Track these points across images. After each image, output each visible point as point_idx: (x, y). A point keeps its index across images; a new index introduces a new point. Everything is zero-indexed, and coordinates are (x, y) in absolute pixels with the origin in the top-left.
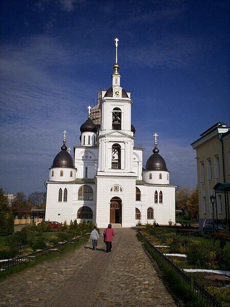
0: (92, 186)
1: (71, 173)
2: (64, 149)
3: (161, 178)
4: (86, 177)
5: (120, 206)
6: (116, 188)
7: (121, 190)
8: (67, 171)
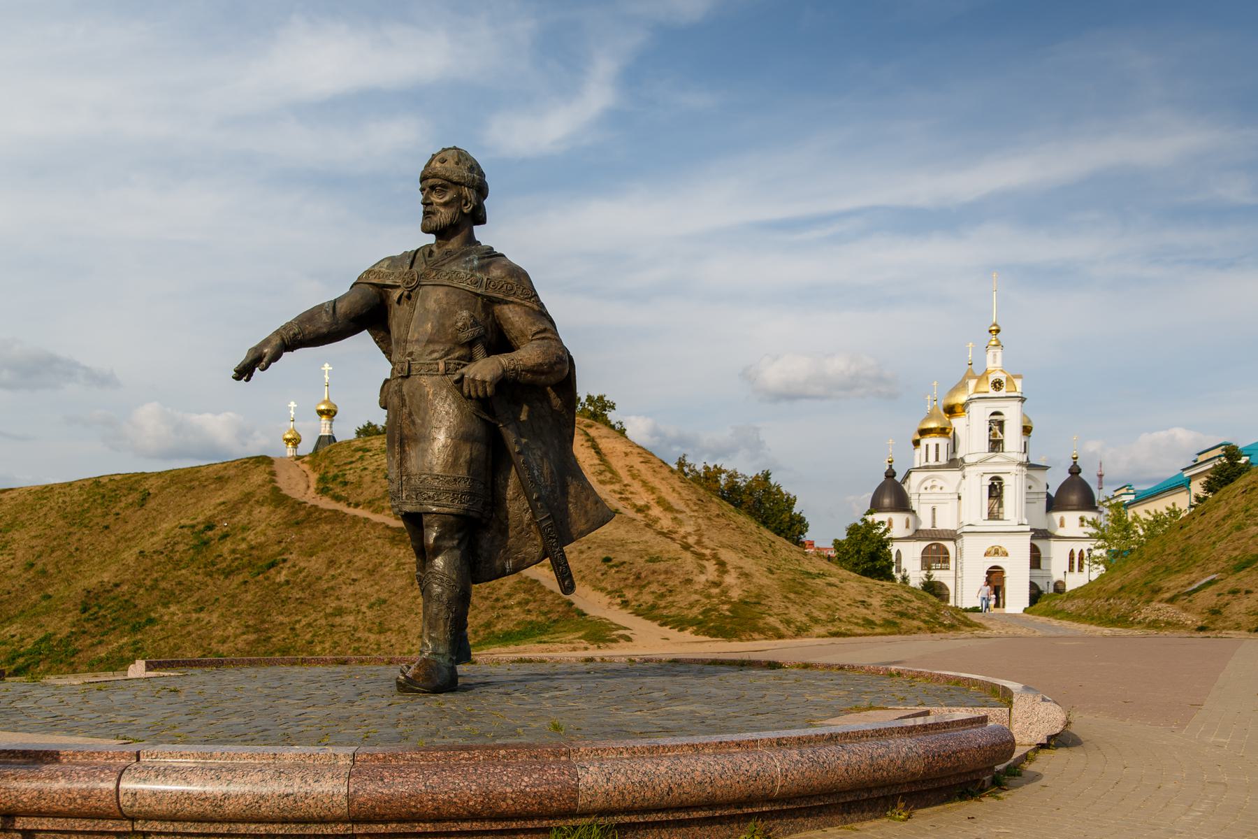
5: (1002, 579)
6: (997, 552)
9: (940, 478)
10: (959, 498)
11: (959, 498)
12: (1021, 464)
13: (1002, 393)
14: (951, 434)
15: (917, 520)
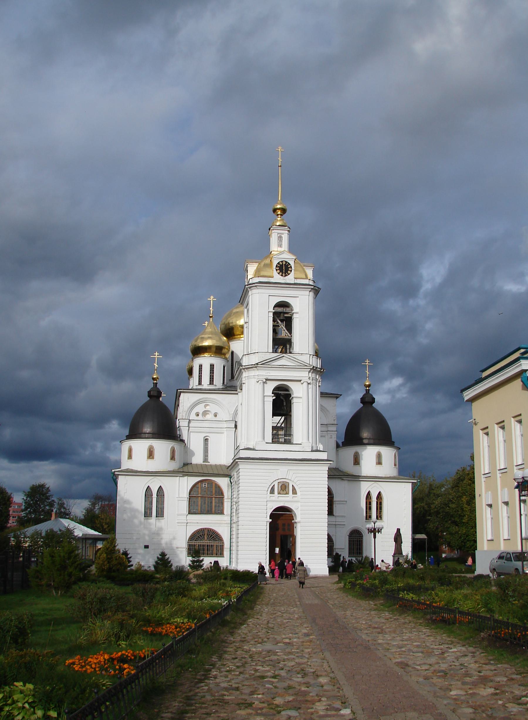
0: (223, 482)
1: (173, 452)
2: (155, 394)
3: (379, 463)
4: (206, 460)
6: (284, 488)
7: (294, 492)
8: (162, 447)
9: (214, 402)
10: (236, 427)
11: (236, 427)
12: (314, 370)
13: (290, 278)
14: (228, 356)
15: (187, 451)
